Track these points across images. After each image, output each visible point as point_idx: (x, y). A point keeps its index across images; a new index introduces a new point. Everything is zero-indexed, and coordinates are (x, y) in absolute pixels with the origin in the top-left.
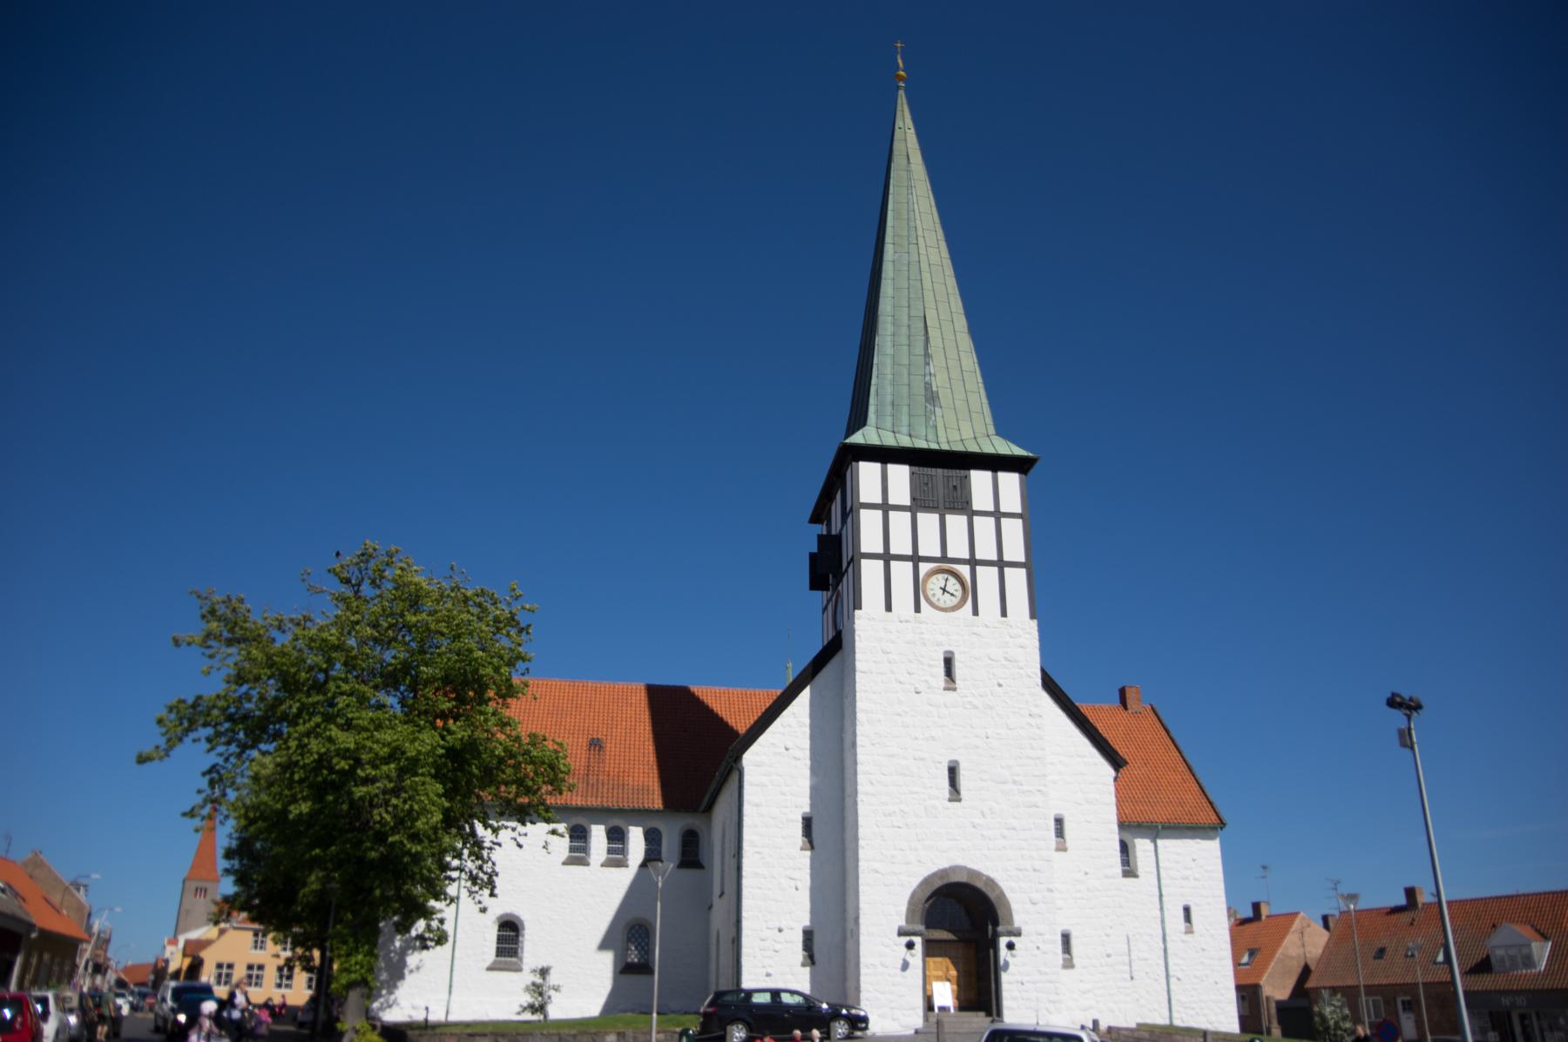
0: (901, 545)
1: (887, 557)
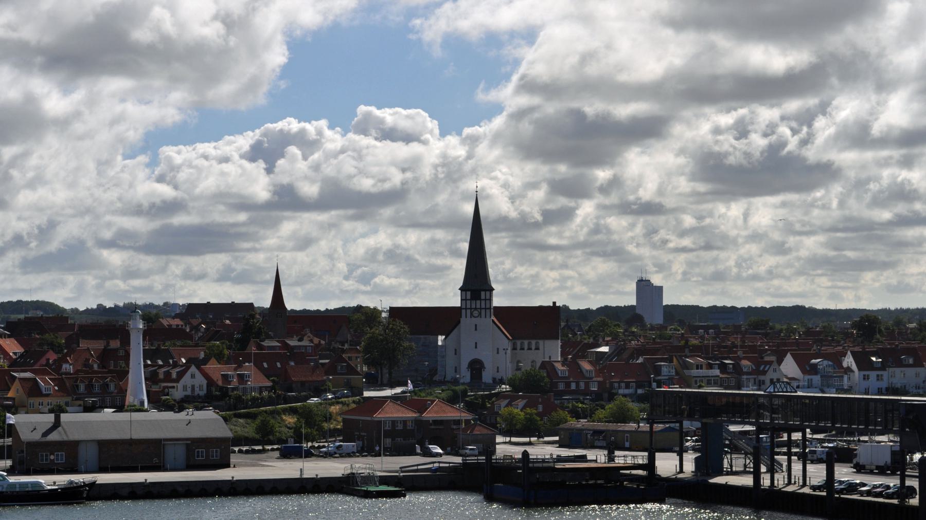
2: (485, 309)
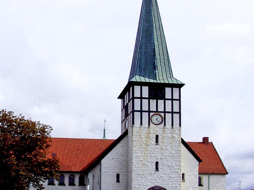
0: (145, 108)
1: (141, 111)
2: (172, 113)
